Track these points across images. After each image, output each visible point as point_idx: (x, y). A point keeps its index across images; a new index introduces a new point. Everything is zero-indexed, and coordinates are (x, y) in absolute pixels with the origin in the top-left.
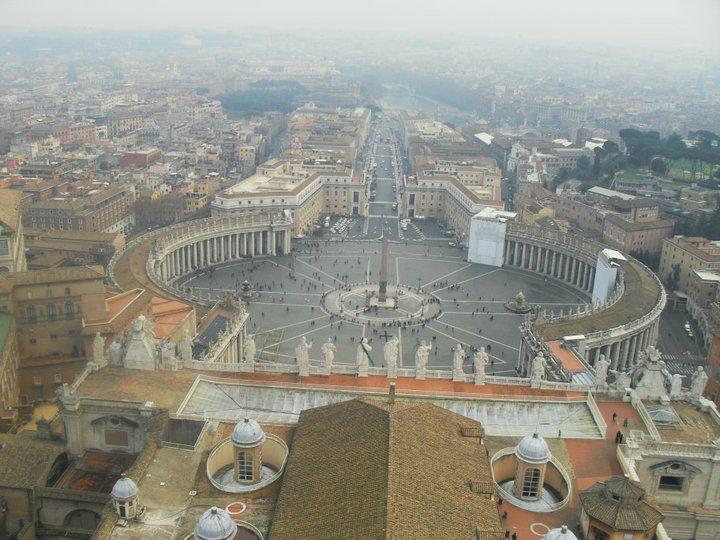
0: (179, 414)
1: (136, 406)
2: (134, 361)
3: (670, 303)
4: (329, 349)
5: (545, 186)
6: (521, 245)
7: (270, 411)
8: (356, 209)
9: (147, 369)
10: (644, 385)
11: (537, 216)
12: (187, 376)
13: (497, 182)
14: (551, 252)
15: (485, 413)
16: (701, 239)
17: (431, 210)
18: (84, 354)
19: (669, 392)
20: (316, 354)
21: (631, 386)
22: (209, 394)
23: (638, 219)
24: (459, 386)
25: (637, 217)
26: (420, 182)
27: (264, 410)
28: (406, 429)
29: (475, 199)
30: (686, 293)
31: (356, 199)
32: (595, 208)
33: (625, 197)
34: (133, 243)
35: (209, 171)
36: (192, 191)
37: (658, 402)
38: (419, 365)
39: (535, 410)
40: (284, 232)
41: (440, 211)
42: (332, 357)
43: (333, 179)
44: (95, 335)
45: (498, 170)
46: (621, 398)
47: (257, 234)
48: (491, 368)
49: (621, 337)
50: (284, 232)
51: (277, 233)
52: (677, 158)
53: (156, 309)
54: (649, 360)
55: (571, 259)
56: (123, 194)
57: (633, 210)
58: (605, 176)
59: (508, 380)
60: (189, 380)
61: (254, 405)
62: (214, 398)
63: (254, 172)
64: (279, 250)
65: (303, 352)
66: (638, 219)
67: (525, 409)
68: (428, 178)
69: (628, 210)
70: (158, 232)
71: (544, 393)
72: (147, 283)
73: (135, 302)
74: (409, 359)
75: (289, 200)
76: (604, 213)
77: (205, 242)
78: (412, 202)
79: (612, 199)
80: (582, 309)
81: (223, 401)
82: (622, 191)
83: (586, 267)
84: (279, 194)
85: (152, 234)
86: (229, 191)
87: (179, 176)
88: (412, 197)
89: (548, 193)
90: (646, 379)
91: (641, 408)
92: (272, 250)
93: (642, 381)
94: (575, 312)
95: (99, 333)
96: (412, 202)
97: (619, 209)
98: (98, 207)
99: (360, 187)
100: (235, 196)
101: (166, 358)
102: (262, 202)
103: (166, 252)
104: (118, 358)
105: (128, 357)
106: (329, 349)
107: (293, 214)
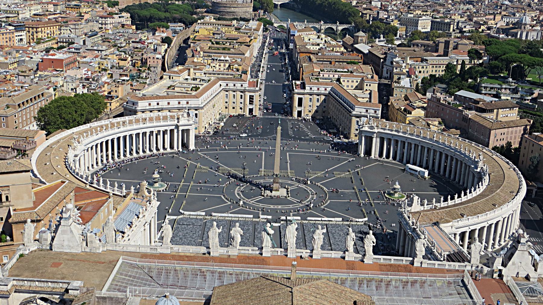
0: (104, 292)
1: (65, 286)
3: (528, 191)
4: (237, 232)
5: (417, 90)
6: (397, 142)
7: (186, 288)
8: (251, 111)
9: (73, 251)
10: (513, 264)
11: (409, 117)
12: (111, 258)
13: (375, 87)
14: (422, 146)
15: (374, 288)
18: (12, 240)
19: (536, 270)
20: (227, 240)
21: (502, 265)
22: (129, 274)
23: (499, 119)
24: (351, 266)
25: (500, 116)
26: (308, 88)
27: (180, 287)
28: (307, 301)
31: (251, 102)
32: (460, 108)
33: (488, 99)
34: (53, 139)
35: (121, 75)
36: (106, 93)
37: (527, 278)
38: (315, 247)
39: (418, 285)
40: (188, 131)
41: (324, 112)
42: (239, 239)
43: (231, 85)
44: (25, 222)
45: (376, 77)
47: (165, 132)
48: (376, 251)
50: (188, 131)
51: (183, 131)
52: (532, 65)
54: (519, 242)
55: (441, 153)
56: (42, 94)
57: (495, 111)
58: (470, 80)
59: (393, 259)
60: (113, 261)
61: (170, 283)
62: (134, 277)
63: (161, 78)
64: (185, 145)
65: (214, 234)
66: (499, 119)
67: (409, 284)
68: (315, 84)
69: (491, 111)
70: (75, 130)
71: (427, 270)
73: (59, 192)
74: (304, 240)
75: (193, 103)
76: (471, 114)
77: (119, 138)
78: (300, 104)
79: (476, 102)
80: (452, 198)
81: (143, 279)
82: (485, 94)
83: (454, 162)
84: (185, 97)
85: (69, 132)
86: (140, 94)
88: (300, 100)
91: (512, 284)
92: (178, 147)
94: (446, 200)
95: (29, 220)
96: (300, 104)
98: (19, 105)
99: (255, 91)
101: (91, 242)
102: (169, 103)
106: (237, 232)
107: (196, 114)
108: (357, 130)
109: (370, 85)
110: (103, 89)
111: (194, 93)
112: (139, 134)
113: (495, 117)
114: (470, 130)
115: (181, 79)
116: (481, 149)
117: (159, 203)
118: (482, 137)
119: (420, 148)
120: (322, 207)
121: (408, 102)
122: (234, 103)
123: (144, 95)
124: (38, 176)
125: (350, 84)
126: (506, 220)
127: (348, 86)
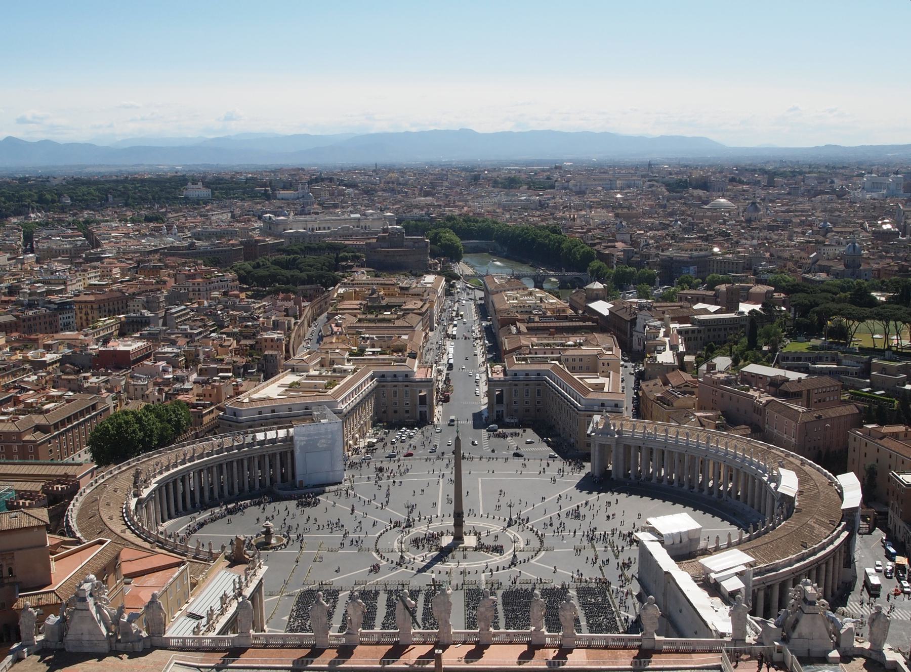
2: (80, 641)
5: (683, 366)
10: (800, 637)
14: (693, 458)
16: (901, 428)
17: (528, 411)
29: (584, 390)
30: (887, 505)
33: (793, 376)
41: (538, 411)
45: (618, 352)
46: (771, 656)
49: (792, 572)
53: (127, 568)
56: (94, 407)
58: (765, 348)
60: (160, 664)
72: (123, 531)
82: (789, 369)
85: (133, 461)
87: (177, 379)
89: (687, 377)
90: (804, 627)
93: (798, 630)
97: (787, 395)
98: (56, 426)
100: (251, 401)
103: (153, 486)
104: (57, 639)
105: (69, 637)
108: (589, 436)
109: (608, 364)
110: (190, 392)
111: (330, 392)
112: (242, 460)
113: (805, 403)
114: (767, 426)
115: (313, 373)
116: (783, 455)
117: (265, 568)
118: (785, 436)
119: (686, 458)
120: (532, 561)
121: (669, 388)
122: (395, 404)
123: (251, 401)
124: (78, 535)
125: (577, 364)
126: (824, 567)
127: (574, 368)
